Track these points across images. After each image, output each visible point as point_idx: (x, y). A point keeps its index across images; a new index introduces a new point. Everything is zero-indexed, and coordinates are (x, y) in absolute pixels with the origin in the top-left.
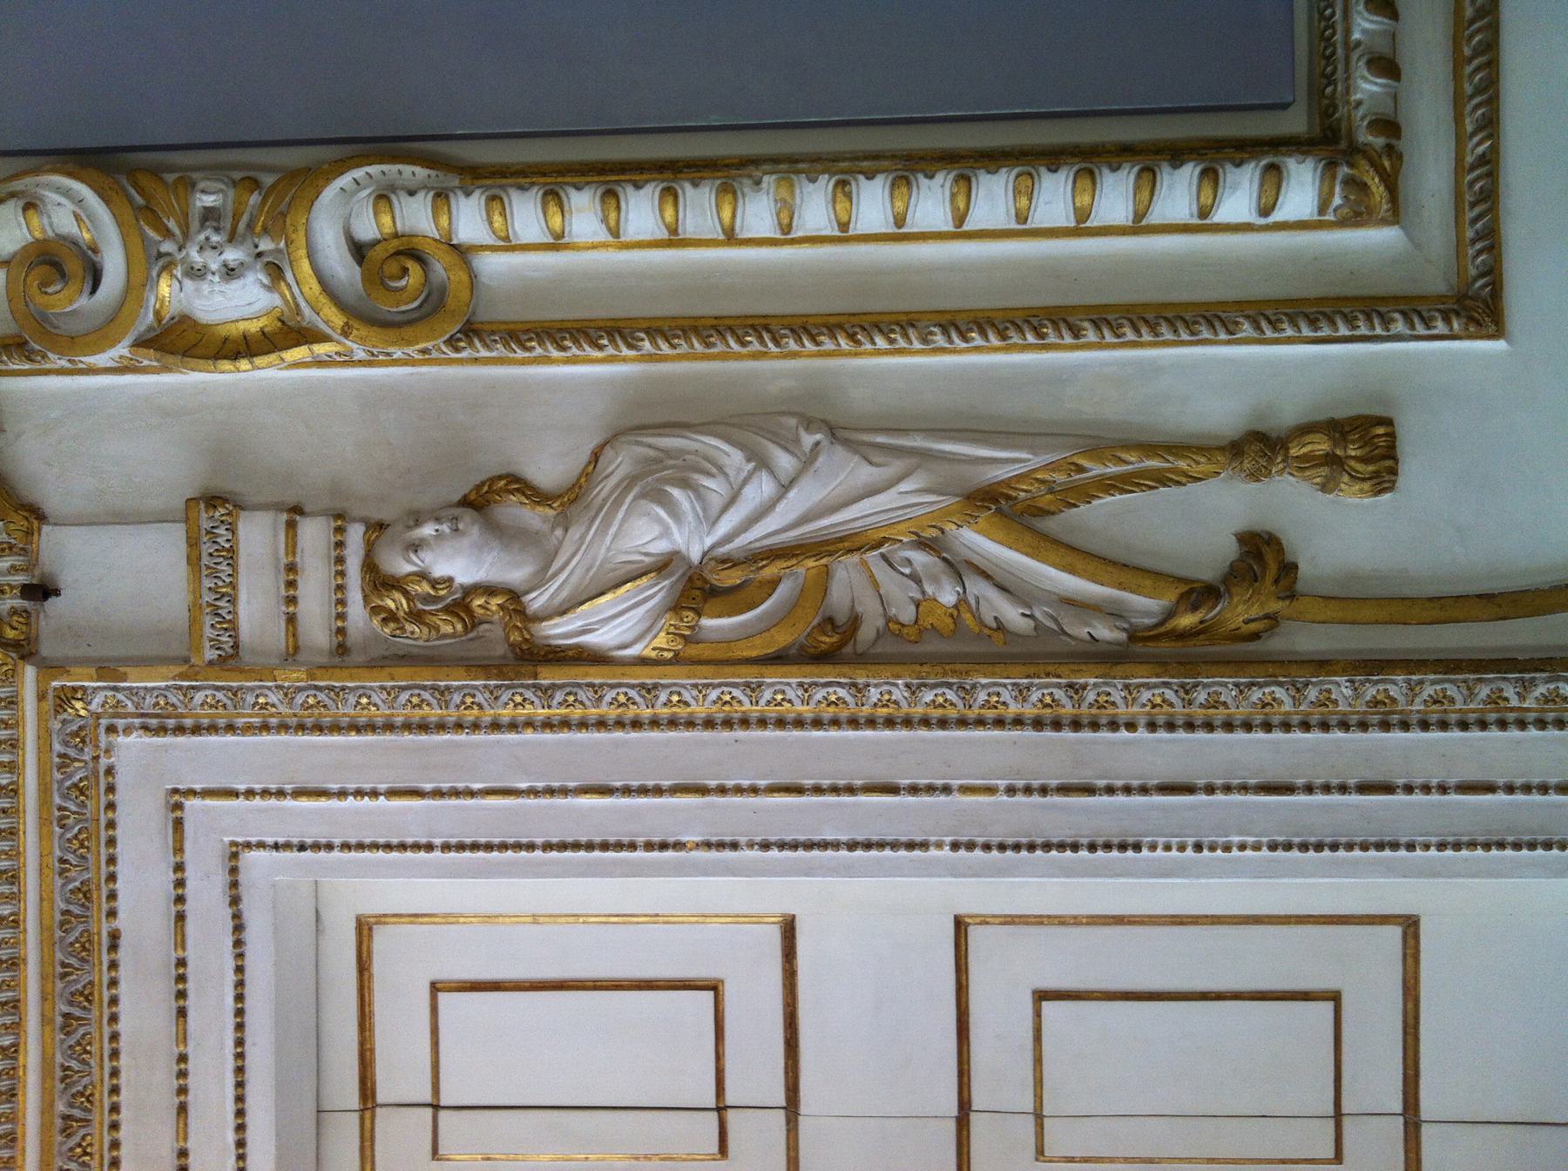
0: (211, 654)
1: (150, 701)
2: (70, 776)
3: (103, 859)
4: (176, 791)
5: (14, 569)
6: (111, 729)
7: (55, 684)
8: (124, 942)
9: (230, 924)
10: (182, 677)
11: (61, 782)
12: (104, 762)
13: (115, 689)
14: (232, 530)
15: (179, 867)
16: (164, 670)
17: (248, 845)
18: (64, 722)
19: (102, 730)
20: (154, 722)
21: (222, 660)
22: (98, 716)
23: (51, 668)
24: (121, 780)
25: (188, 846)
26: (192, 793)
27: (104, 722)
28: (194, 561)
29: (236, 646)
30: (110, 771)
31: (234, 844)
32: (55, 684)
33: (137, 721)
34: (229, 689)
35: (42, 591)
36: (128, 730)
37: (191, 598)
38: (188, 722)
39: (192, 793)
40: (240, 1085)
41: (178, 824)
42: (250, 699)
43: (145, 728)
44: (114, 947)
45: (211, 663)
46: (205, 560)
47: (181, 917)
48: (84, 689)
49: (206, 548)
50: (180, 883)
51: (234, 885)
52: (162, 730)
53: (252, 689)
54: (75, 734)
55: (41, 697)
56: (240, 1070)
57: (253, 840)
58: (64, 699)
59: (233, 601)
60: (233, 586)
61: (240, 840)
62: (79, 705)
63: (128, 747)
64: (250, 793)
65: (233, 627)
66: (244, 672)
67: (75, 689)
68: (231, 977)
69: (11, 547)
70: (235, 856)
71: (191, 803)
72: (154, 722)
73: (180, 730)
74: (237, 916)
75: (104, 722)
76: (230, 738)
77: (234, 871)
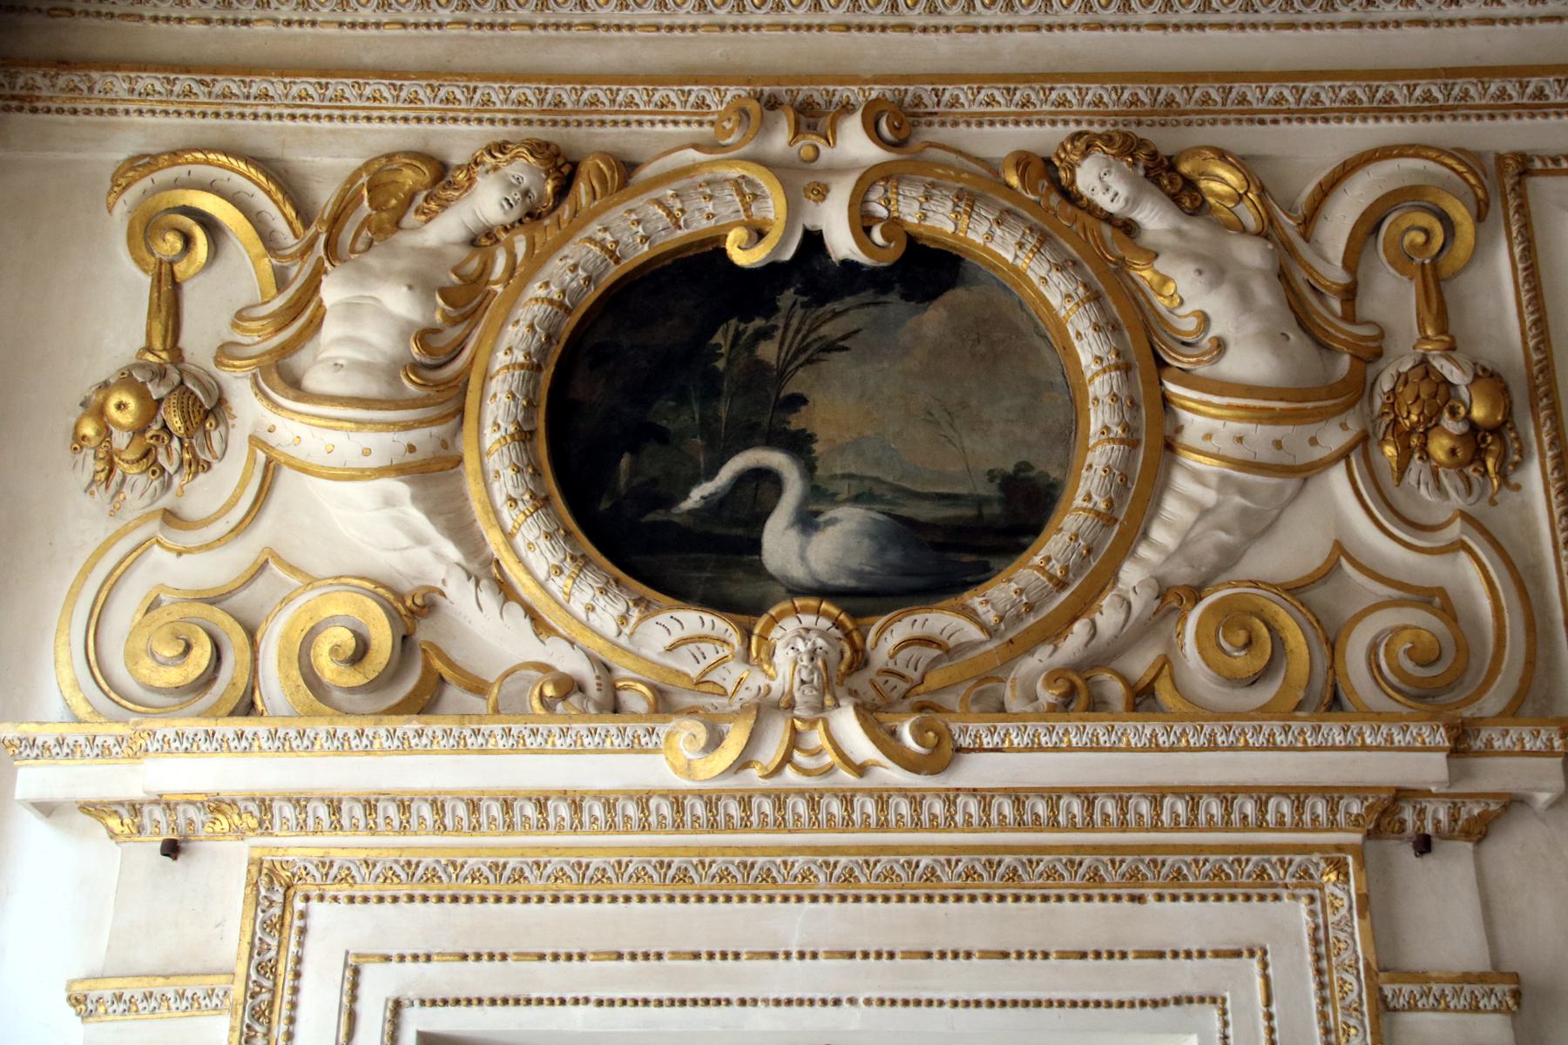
0: (1388, 990)
1: (1342, 936)
2: (1273, 866)
3: (1204, 891)
4: (1265, 953)
5: (1437, 822)
6: (1312, 899)
7: (1350, 859)
8: (1136, 905)
9: (1158, 996)
10: (1367, 966)
11: (1269, 861)
12: (1284, 893)
13: (1350, 908)
14: (1495, 1010)
15: (1202, 954)
16: (1372, 950)
17: (1224, 1012)
18: (1317, 865)
19: (1310, 891)
20: (1321, 934)
21: (1384, 999)
22: (1321, 889)
23: (1359, 852)
24: (1270, 904)
25: (1219, 961)
26: (1265, 966)
27: (1317, 893)
28: (1466, 978)
29: (1395, 1010)
30: (1277, 898)
31: (1224, 1000)
32: (1350, 859)
33: (1320, 921)
34: (1361, 1004)
35: (1424, 845)
36: (1313, 913)
37: (1434, 975)
38: (1324, 964)
39: (1265, 966)
40: (1026, 1004)
41: (1237, 954)
42: (1352, 1022)
43: (1316, 928)
44: (1132, 898)
45: (1381, 989)
46: (1467, 988)
47: (1160, 955)
48: (1347, 881)
49: (1478, 989)
50: (1188, 955)
51: (1190, 1000)
52: (1316, 942)
53: (1362, 1022)
54: (1306, 871)
55: (1339, 848)
56: (1038, 1004)
57: (1229, 1017)
58: (1339, 867)
59: (1434, 1009)
60: (1447, 1009)
61: (1228, 1005)
62: (1333, 877)
63: (1297, 912)
64: (1270, 1017)
65: (1412, 1007)
66: (1375, 1020)
67: (1347, 875)
68: (1115, 997)
69: (1456, 821)
70: (1214, 1001)
71: (1255, 965)
72: (1321, 934)
73: (1318, 957)
74: (1165, 1002)
75: (1317, 893)
76: (1314, 1001)
77: (1202, 1000)
